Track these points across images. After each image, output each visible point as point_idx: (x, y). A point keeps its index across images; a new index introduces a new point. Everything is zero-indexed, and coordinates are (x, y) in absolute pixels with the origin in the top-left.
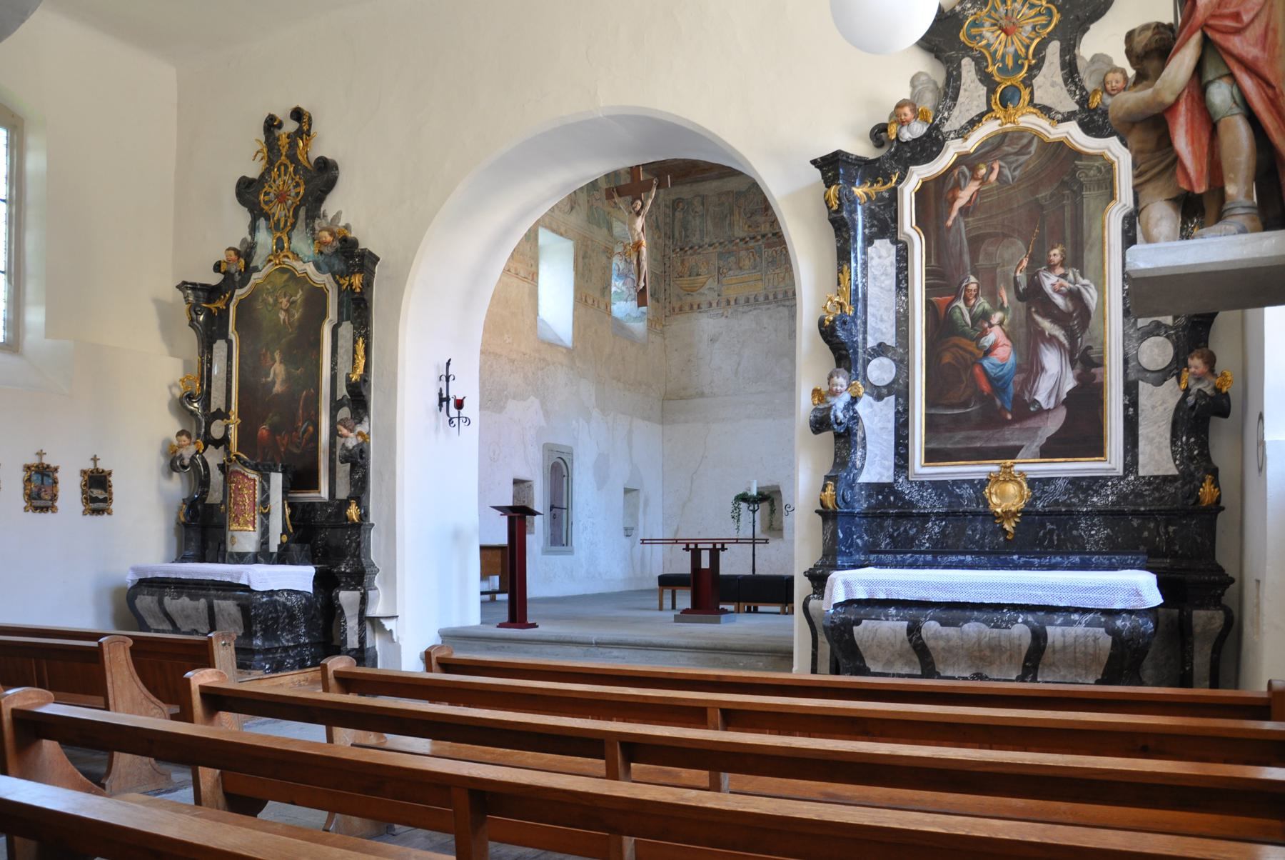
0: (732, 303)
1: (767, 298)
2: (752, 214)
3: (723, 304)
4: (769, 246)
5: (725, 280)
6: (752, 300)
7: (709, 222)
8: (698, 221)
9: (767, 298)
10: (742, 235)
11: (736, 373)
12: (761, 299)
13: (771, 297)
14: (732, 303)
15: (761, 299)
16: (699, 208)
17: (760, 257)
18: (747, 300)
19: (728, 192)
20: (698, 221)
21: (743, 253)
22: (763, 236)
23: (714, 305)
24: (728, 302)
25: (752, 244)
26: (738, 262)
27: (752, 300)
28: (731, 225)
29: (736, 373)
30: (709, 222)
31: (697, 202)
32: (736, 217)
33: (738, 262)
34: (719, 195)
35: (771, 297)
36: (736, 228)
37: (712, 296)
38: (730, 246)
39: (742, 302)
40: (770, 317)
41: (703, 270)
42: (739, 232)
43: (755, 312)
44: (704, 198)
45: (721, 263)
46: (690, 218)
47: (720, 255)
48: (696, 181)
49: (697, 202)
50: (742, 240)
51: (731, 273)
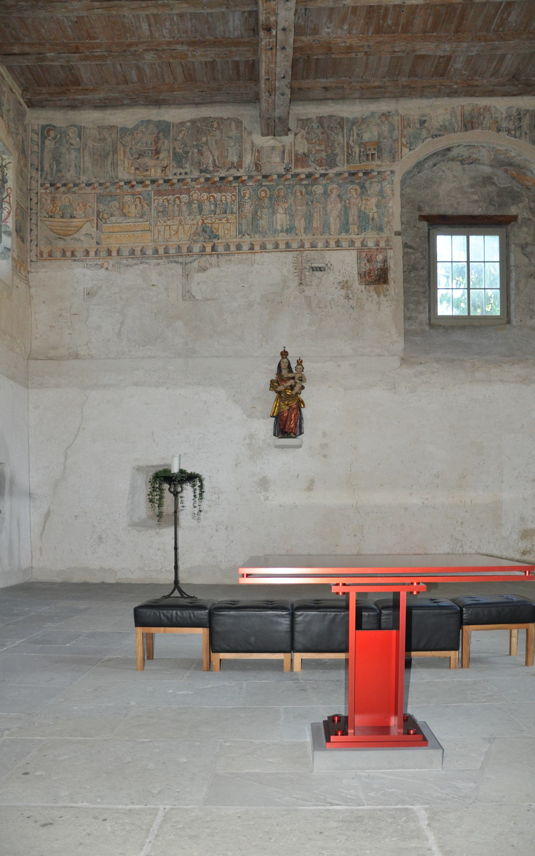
0: (114, 253)
1: (156, 251)
2: (141, 155)
3: (103, 254)
4: (159, 193)
5: (105, 227)
6: (138, 253)
7: (87, 158)
8: (73, 154)
9: (156, 251)
10: (127, 177)
11: (119, 334)
12: (149, 252)
13: (161, 251)
14: (114, 253)
15: (149, 252)
16: (75, 141)
17: (149, 205)
18: (132, 252)
19: (111, 128)
20: (73, 154)
21: (128, 198)
22: (153, 182)
23: (92, 253)
24: (109, 253)
25: (139, 188)
26: (122, 208)
27: (138, 253)
28: (114, 165)
29: (119, 334)
30: (87, 158)
31: (72, 133)
32: (120, 156)
33: (122, 208)
34: (101, 128)
35: (161, 251)
36: (120, 169)
37: (90, 244)
38: (112, 189)
39: (126, 253)
40: (160, 274)
41: (79, 212)
42: (124, 173)
43: (141, 267)
44: (80, 131)
45: (101, 207)
46: (64, 150)
47: (100, 198)
48: (73, 107)
49: (72, 133)
50: (127, 183)
51: (113, 219)
